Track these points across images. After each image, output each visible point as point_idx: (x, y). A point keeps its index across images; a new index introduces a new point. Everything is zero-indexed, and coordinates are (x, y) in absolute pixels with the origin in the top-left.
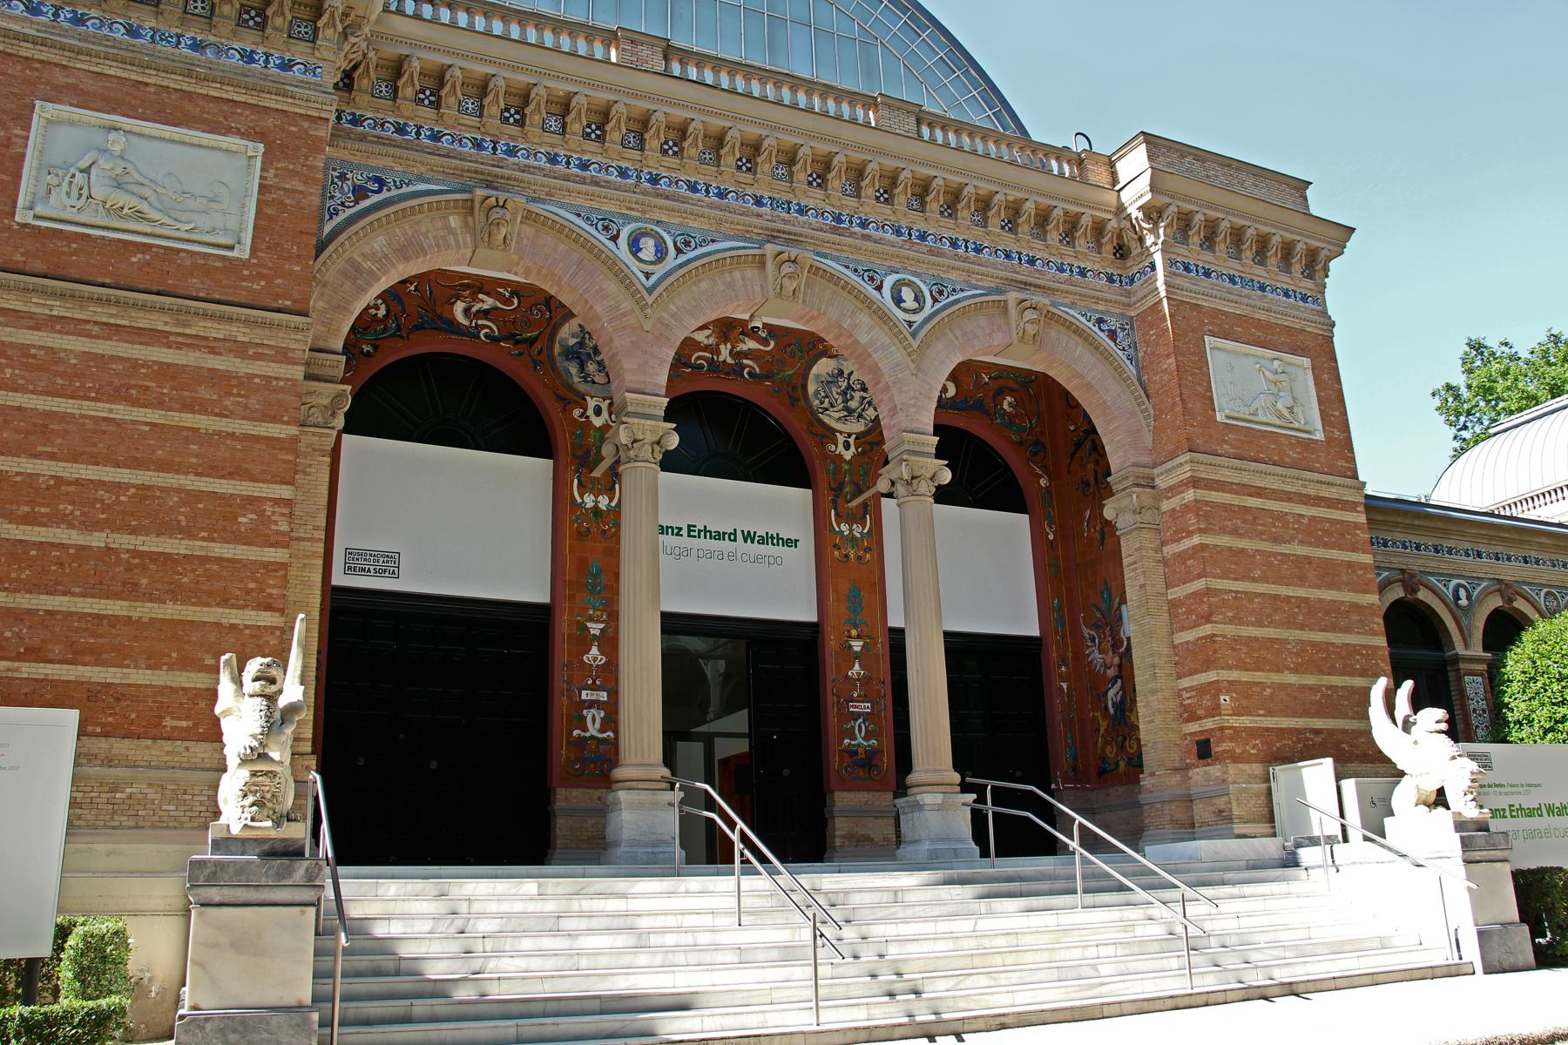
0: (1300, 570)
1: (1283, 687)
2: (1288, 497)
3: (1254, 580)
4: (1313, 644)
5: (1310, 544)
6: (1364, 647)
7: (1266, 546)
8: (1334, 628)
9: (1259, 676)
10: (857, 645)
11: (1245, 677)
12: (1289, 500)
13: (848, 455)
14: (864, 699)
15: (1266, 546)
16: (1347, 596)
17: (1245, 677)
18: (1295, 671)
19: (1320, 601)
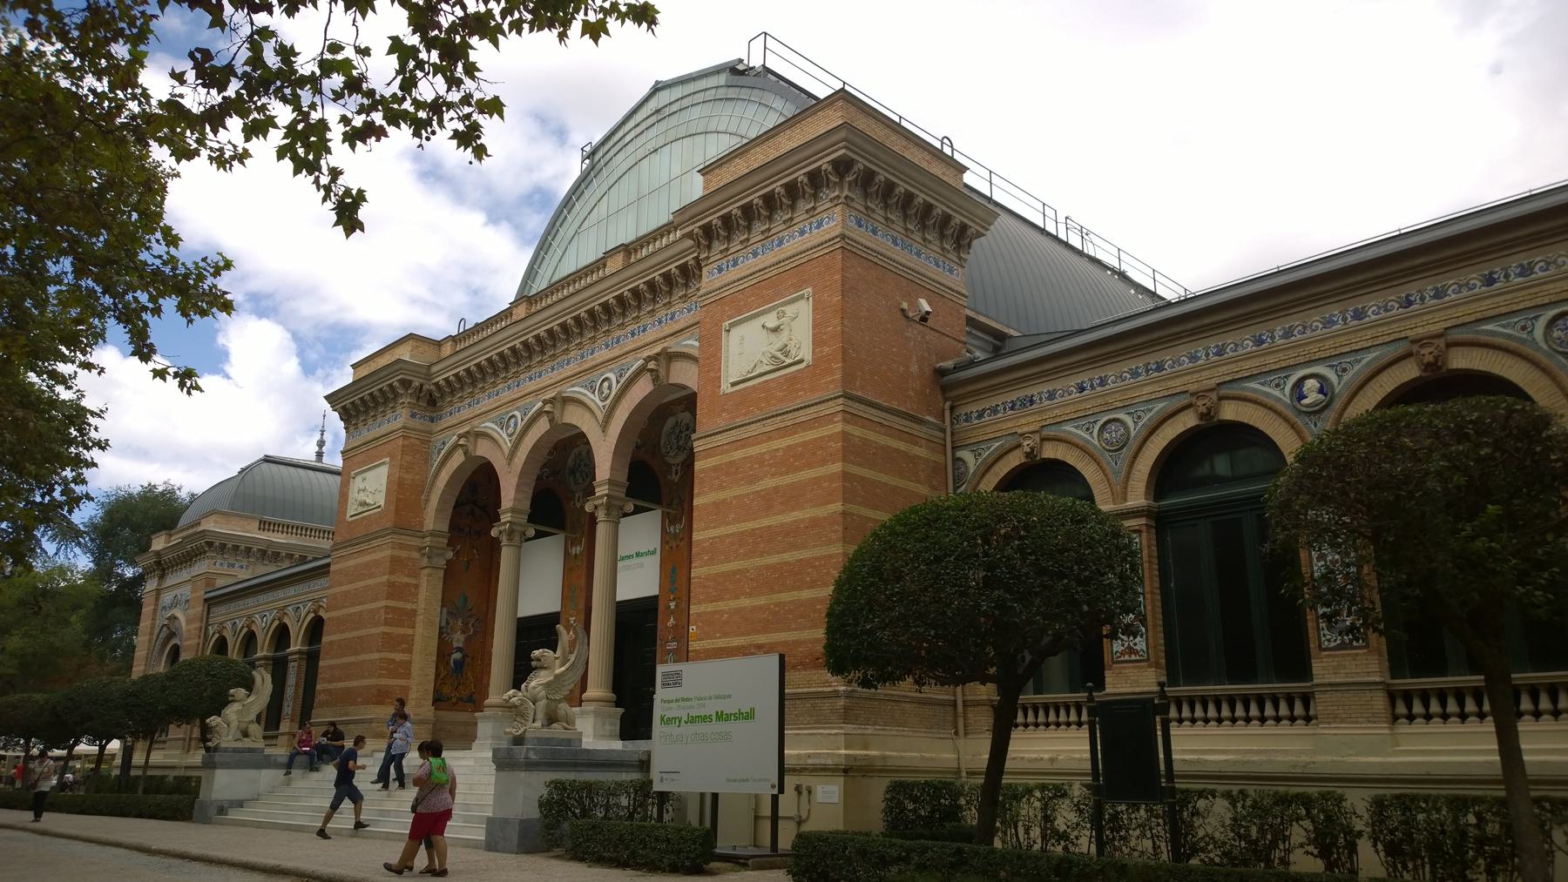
0: (768, 501)
1: (738, 611)
2: (769, 437)
3: (728, 524)
4: (768, 567)
5: (782, 474)
6: (817, 559)
7: (744, 490)
8: (793, 547)
9: (721, 605)
10: (673, 605)
11: (710, 608)
12: (770, 439)
13: (676, 479)
14: (674, 639)
15: (744, 490)
16: (809, 513)
17: (710, 608)
18: (750, 595)
19: (782, 525)
